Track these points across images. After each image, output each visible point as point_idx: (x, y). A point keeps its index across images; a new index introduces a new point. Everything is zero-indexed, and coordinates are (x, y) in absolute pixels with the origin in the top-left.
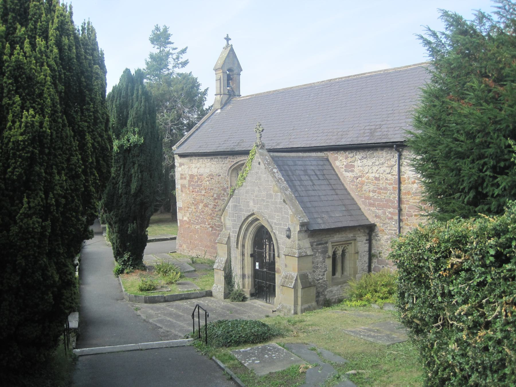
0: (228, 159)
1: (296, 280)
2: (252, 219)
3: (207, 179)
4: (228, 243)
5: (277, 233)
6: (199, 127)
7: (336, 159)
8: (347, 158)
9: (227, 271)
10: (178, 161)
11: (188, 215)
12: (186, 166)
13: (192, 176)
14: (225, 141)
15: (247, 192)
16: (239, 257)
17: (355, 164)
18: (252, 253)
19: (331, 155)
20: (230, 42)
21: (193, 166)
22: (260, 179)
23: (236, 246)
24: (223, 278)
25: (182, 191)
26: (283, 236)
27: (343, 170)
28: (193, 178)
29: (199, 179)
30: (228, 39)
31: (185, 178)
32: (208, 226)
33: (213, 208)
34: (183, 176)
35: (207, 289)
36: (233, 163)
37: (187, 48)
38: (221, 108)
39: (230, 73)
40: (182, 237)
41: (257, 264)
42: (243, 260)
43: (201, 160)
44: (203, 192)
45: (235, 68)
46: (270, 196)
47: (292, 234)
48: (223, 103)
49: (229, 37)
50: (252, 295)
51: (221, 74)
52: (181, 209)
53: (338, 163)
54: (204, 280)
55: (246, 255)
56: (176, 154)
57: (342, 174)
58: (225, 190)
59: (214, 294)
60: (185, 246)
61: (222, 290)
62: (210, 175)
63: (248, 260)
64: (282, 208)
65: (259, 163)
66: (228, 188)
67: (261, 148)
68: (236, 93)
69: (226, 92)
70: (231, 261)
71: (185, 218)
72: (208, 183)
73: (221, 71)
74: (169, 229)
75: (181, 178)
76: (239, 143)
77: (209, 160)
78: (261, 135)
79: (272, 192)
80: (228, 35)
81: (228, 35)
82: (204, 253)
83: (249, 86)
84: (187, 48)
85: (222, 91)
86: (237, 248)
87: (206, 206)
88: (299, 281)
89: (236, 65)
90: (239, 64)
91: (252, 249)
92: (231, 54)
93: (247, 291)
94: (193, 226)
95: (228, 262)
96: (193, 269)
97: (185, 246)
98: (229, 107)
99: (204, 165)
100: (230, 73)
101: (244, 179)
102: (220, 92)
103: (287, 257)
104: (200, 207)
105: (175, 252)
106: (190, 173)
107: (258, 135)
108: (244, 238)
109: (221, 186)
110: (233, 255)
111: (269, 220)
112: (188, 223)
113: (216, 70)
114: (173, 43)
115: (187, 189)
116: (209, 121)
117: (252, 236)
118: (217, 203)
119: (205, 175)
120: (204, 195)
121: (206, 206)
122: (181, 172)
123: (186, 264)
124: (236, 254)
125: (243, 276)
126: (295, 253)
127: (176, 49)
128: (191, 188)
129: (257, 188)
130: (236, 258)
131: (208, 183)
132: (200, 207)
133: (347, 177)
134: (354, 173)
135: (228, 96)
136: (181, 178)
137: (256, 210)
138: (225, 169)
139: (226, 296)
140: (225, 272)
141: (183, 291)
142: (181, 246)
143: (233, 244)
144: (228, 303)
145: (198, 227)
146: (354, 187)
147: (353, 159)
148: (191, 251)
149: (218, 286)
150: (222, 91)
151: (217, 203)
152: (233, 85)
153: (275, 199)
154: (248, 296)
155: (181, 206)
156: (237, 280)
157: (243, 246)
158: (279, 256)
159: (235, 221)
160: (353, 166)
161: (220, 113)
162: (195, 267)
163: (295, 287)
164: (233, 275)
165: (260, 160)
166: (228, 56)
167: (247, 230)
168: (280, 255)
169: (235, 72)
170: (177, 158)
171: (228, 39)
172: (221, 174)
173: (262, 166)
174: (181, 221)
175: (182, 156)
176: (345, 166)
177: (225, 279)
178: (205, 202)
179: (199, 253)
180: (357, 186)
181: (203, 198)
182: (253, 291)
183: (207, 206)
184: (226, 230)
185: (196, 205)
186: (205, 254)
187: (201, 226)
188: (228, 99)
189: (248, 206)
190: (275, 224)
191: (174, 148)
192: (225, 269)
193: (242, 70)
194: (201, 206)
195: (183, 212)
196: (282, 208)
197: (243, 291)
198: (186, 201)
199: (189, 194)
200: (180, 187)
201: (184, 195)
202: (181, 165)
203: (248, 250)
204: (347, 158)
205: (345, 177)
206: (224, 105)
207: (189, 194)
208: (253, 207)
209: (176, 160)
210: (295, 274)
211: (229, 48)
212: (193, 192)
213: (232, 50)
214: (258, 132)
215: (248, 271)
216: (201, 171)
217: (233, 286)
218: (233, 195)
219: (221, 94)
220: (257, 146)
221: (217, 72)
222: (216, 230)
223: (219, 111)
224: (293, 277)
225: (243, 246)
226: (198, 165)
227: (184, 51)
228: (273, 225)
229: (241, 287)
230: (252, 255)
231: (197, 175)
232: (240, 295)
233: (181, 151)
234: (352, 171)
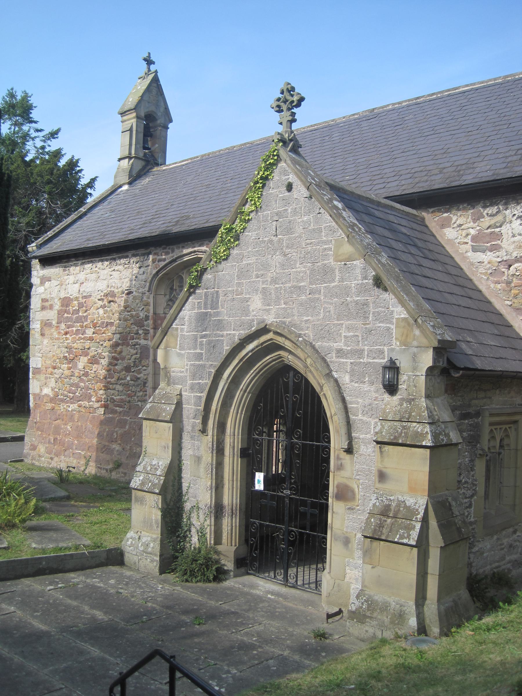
1: (425, 520)
3: (100, 303)
4: (176, 418)
5: (345, 379)
6: (85, 214)
7: (444, 224)
9: (169, 497)
10: (38, 272)
11: (52, 383)
12: (54, 283)
13: (66, 302)
14: (144, 224)
15: (243, 273)
16: (208, 458)
17: (505, 230)
18: (245, 446)
21: (71, 279)
22: (289, 231)
23: (200, 427)
24: (157, 515)
25: (42, 335)
26: (366, 387)
27: (468, 247)
28: (67, 305)
29: (81, 305)
30: (149, 61)
31: (51, 307)
32: (97, 405)
34: (47, 304)
35: (110, 543)
36: (163, 264)
37: (59, 130)
38: (130, 183)
39: (150, 123)
40: (38, 429)
41: (259, 476)
42: (219, 465)
43: (88, 266)
44: (89, 332)
45: (159, 114)
46: (327, 272)
47: (403, 378)
48: (134, 173)
49: (153, 58)
51: (134, 121)
52: (38, 371)
54: (94, 519)
55: (227, 451)
56: (35, 257)
57: (465, 258)
58: (140, 323)
59: (128, 558)
60: (42, 449)
61: (155, 547)
62: (106, 295)
63: (232, 464)
64: (366, 304)
66: (147, 318)
68: (160, 161)
69: (141, 155)
70: (180, 470)
71: (47, 391)
72: (101, 311)
73: (134, 115)
74: (9, 424)
75: (43, 308)
76: (178, 221)
77: (106, 263)
78: (293, 114)
79: (331, 261)
80: (149, 54)
81: (149, 54)
82: (83, 462)
84: (59, 130)
85: (133, 152)
86: (204, 431)
87: (94, 361)
88: (433, 523)
89: (162, 109)
91: (246, 436)
92: (155, 88)
93: (228, 550)
94: (62, 407)
95: (174, 471)
96: (62, 493)
97: (42, 449)
98: (146, 181)
99: (94, 276)
100: (150, 123)
101: (237, 238)
102: (130, 153)
103: (387, 448)
104: (80, 365)
105: (22, 461)
106: (63, 295)
108: (226, 404)
109: (132, 316)
110: (187, 453)
111: (318, 345)
112: (52, 400)
114: (36, 122)
115: (53, 330)
116: (106, 203)
117: (247, 398)
118: (121, 352)
120: (91, 339)
121: (94, 361)
122: (43, 296)
123: (46, 482)
124: (197, 450)
125: (218, 510)
126: (423, 436)
127: (41, 130)
128: (63, 326)
129: (278, 258)
130: (198, 459)
131: (101, 311)
132: (80, 365)
133: (478, 264)
134: (502, 253)
136: (43, 308)
137: (270, 319)
138: (144, 277)
139: (168, 563)
140: (164, 500)
141: (44, 551)
142: (34, 448)
144: (172, 587)
145: (73, 407)
146: (499, 286)
147: (499, 218)
148: (56, 459)
149: (141, 535)
150: (133, 152)
151: (121, 352)
152: (153, 145)
153: (342, 280)
154: (229, 565)
155: (39, 366)
156: (199, 522)
157: (221, 427)
158: (349, 450)
159: (199, 357)
160: (499, 236)
161: (128, 190)
162: (66, 490)
163: (422, 545)
164: (187, 506)
165: (292, 178)
166: (148, 89)
167: (235, 381)
168: (355, 446)
169: (159, 122)
170: (35, 263)
171: (149, 61)
172: (133, 290)
173: (300, 191)
175: (48, 261)
176: (474, 239)
177: (164, 517)
178: (91, 354)
179: (74, 462)
180: (508, 283)
181: (87, 344)
182: (244, 551)
183: (97, 363)
184: (168, 384)
185: (71, 361)
186: (87, 464)
187: (80, 406)
188: (144, 168)
189: (246, 311)
190: (340, 352)
191: (32, 247)
192: (163, 492)
193: (171, 121)
194: (82, 362)
195: (42, 377)
196: (366, 304)
197: (217, 552)
198: (51, 354)
199: (58, 339)
200: (38, 326)
201: (46, 341)
202: (44, 280)
203: (234, 439)
205: (472, 264)
206: (134, 177)
207: (58, 339)
208: (260, 310)
209: (34, 273)
210: (419, 502)
211: (151, 77)
212: (66, 333)
213: (156, 80)
215: (231, 497)
216: (88, 287)
217: (185, 537)
218: (197, 287)
219: (130, 158)
221: (125, 118)
222: (115, 412)
223: (126, 187)
224: (414, 512)
225: (221, 427)
226: (82, 276)
227: (54, 135)
228: (331, 358)
229: (210, 539)
230: (244, 453)
231: (77, 298)
232: (208, 563)
233: (46, 250)
234: (495, 248)
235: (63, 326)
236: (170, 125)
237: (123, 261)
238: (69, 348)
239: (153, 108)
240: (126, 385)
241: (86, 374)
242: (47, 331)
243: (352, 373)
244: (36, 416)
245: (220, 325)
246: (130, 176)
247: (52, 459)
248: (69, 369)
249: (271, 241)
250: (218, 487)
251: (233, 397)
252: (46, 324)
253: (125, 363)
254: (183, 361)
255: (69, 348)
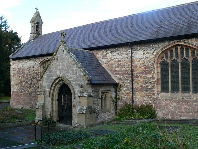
0: (39, 59)
2: (59, 80)
4: (44, 95)
5: (74, 86)
7: (97, 54)
8: (103, 53)
10: (12, 62)
13: (19, 69)
16: (51, 102)
17: (108, 55)
19: (94, 52)
20: (38, 11)
21: (20, 64)
22: (64, 59)
26: (77, 87)
29: (23, 70)
30: (37, 9)
33: (30, 83)
38: (33, 40)
39: (37, 23)
44: (25, 76)
46: (70, 67)
48: (34, 37)
50: (58, 121)
52: (12, 85)
53: (98, 56)
55: (54, 100)
56: (11, 59)
58: (37, 74)
60: (14, 104)
65: (64, 51)
66: (38, 73)
67: (64, 43)
72: (28, 71)
75: (14, 71)
79: (71, 65)
83: (46, 30)
87: (27, 82)
89: (41, 21)
90: (42, 21)
91: (58, 97)
92: (38, 15)
93: (55, 118)
95: (44, 104)
97: (14, 104)
100: (37, 23)
103: (80, 97)
104: (23, 84)
106: (18, 68)
107: (63, 37)
108: (53, 91)
111: (69, 80)
113: (31, 22)
117: (58, 90)
118: (33, 81)
119: (26, 68)
121: (27, 82)
124: (49, 100)
128: (19, 75)
129: (62, 64)
132: (23, 84)
133: (103, 62)
134: (107, 60)
135: (36, 35)
136: (14, 71)
137: (61, 75)
142: (12, 104)
143: (48, 95)
146: (107, 66)
147: (107, 53)
150: (34, 32)
151: (33, 81)
157: (53, 95)
159: (48, 82)
160: (107, 56)
165: (64, 49)
166: (37, 16)
171: (37, 9)
173: (65, 52)
174: (13, 92)
175: (14, 59)
176: (102, 57)
180: (108, 65)
183: (27, 83)
185: (21, 83)
188: (37, 35)
189: (57, 74)
201: (15, 78)
204: (103, 53)
208: (59, 73)
209: (11, 62)
213: (39, 14)
214: (62, 35)
216: (25, 66)
220: (62, 42)
222: (32, 94)
223: (32, 41)
226: (23, 63)
233: (14, 57)
234: (106, 59)
235: (19, 75)
236: (43, 25)
237: (32, 60)
238: (21, 80)
239: (38, 21)
240: (35, 88)
241: (25, 86)
242: (15, 76)
243: (75, 85)
244: (13, 96)
245: (52, 76)
246: (33, 38)
247: (17, 106)
248: (21, 85)
249: (60, 61)
250: (53, 107)
251: (55, 90)
252: (14, 74)
253: (34, 83)
254: (46, 83)
255: (21, 80)
